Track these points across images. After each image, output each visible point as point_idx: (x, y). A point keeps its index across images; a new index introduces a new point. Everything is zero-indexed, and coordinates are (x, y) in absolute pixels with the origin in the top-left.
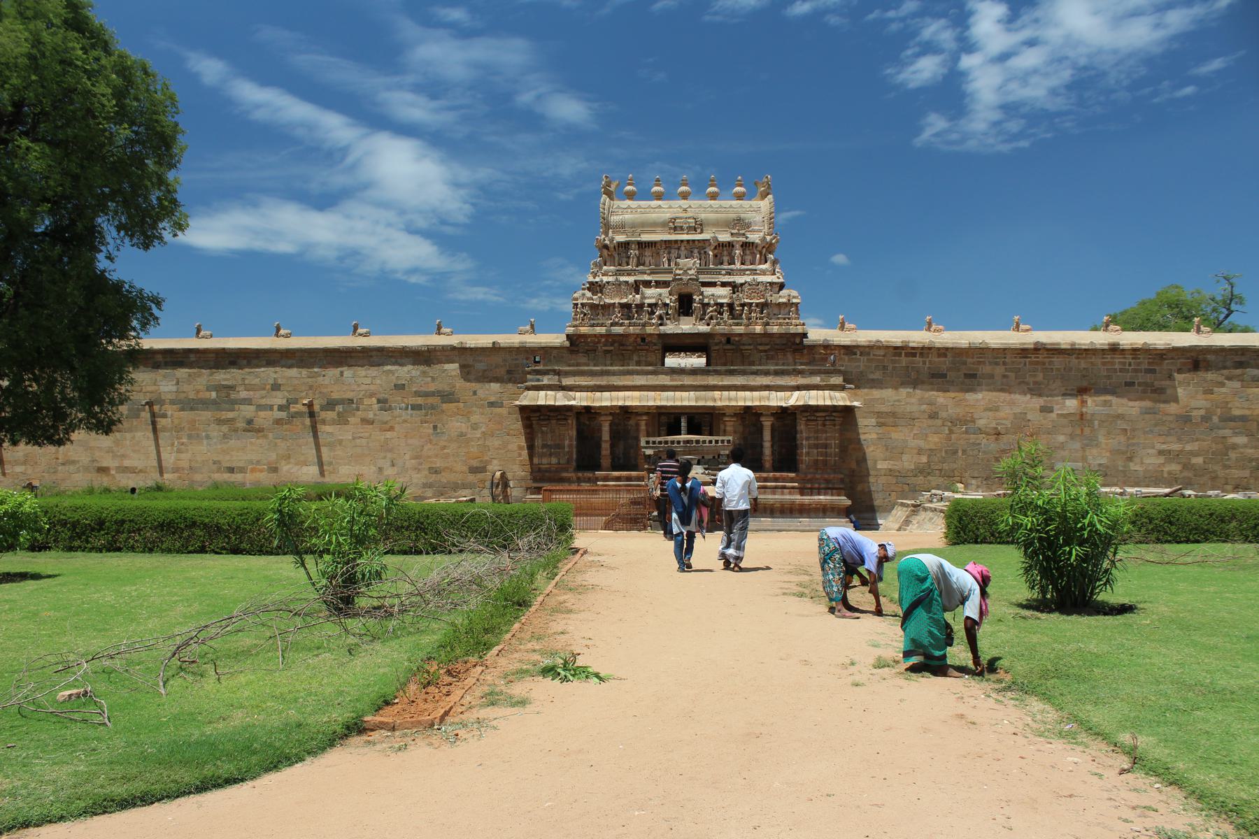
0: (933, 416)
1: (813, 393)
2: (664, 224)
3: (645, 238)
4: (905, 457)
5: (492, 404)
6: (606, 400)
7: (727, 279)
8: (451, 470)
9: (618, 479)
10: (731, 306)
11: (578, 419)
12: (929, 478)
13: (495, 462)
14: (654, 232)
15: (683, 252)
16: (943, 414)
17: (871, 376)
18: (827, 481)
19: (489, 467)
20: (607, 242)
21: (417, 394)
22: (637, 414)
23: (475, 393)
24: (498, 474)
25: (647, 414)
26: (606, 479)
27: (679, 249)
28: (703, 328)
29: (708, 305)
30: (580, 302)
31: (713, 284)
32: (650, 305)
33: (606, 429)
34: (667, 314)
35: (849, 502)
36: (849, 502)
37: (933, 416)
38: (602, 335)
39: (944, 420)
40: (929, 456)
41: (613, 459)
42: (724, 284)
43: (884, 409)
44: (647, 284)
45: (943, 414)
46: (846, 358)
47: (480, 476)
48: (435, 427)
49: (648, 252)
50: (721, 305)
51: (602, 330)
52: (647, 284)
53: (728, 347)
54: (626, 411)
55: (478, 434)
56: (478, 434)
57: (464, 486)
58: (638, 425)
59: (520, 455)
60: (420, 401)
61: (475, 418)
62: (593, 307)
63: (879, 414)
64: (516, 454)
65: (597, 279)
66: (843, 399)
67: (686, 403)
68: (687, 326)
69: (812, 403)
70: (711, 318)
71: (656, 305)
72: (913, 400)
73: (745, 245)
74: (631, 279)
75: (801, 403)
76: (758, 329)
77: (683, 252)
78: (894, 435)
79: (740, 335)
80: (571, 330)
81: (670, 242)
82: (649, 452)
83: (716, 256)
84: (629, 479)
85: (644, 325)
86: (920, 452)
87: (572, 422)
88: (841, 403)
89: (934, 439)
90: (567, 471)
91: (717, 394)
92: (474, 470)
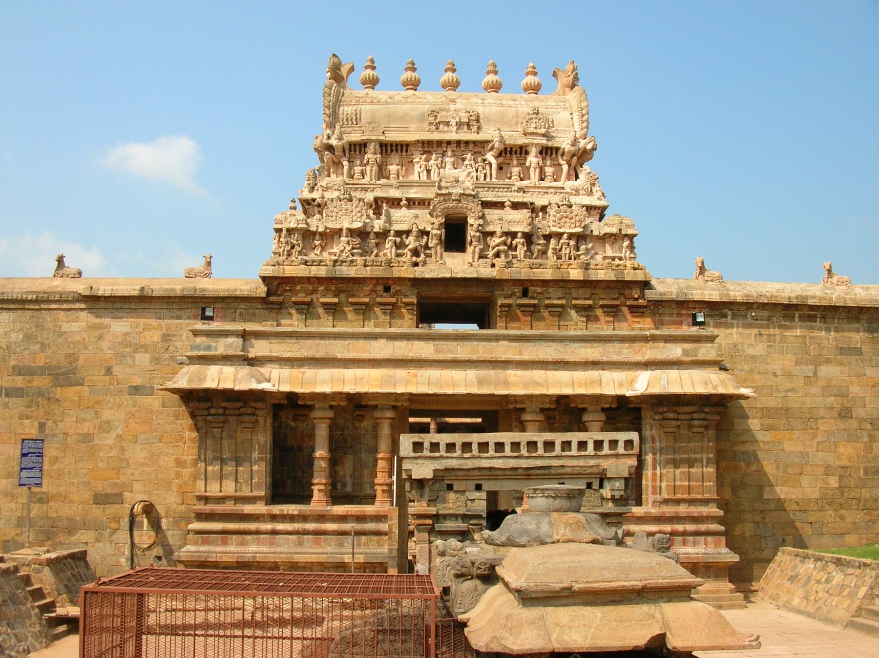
0: (845, 414)
1: (673, 373)
2: (421, 118)
3: (393, 136)
4: (805, 481)
5: (136, 390)
6: (324, 382)
7: (519, 198)
8: (64, 498)
9: (343, 518)
10: (528, 237)
11: (275, 417)
12: (843, 512)
13: (137, 486)
14: (406, 129)
15: (449, 160)
16: (859, 412)
17: (751, 351)
18: (694, 520)
19: (127, 495)
20: (334, 142)
21: (19, 371)
22: (375, 407)
23: (109, 371)
24: (138, 508)
25: (394, 408)
26: (322, 518)
27: (444, 154)
28: (485, 271)
29: (492, 234)
30: (284, 226)
31: (500, 205)
32: (399, 233)
33: (322, 432)
34: (426, 247)
35: (736, 558)
36: (736, 558)
37: (845, 414)
38: (319, 280)
39: (861, 420)
40: (841, 477)
41: (333, 485)
42: (516, 206)
43: (772, 403)
44: (395, 203)
45: (859, 412)
46: (711, 321)
47: (112, 509)
48: (42, 426)
49: (395, 158)
50: (514, 235)
51: (322, 272)
52: (395, 203)
53: (525, 301)
54: (356, 406)
55: (110, 439)
56: (110, 439)
57: (86, 525)
58: (376, 427)
59: (178, 475)
60: (19, 381)
61: (107, 414)
62: (308, 235)
63: (766, 413)
64: (172, 475)
65: (316, 195)
66: (723, 383)
67: (462, 390)
68: (459, 265)
69: (675, 389)
70: (497, 255)
71: (408, 233)
72: (814, 390)
73: (547, 152)
74: (370, 197)
75: (656, 390)
76: (575, 274)
77: (449, 160)
78: (788, 446)
79: (545, 283)
80: (269, 271)
81: (430, 143)
82: (423, 470)
83: (500, 168)
84: (361, 518)
85: (389, 263)
86: (828, 470)
87: (265, 421)
88: (721, 390)
89: (847, 452)
90: (252, 500)
91: (513, 374)
92: (101, 499)
